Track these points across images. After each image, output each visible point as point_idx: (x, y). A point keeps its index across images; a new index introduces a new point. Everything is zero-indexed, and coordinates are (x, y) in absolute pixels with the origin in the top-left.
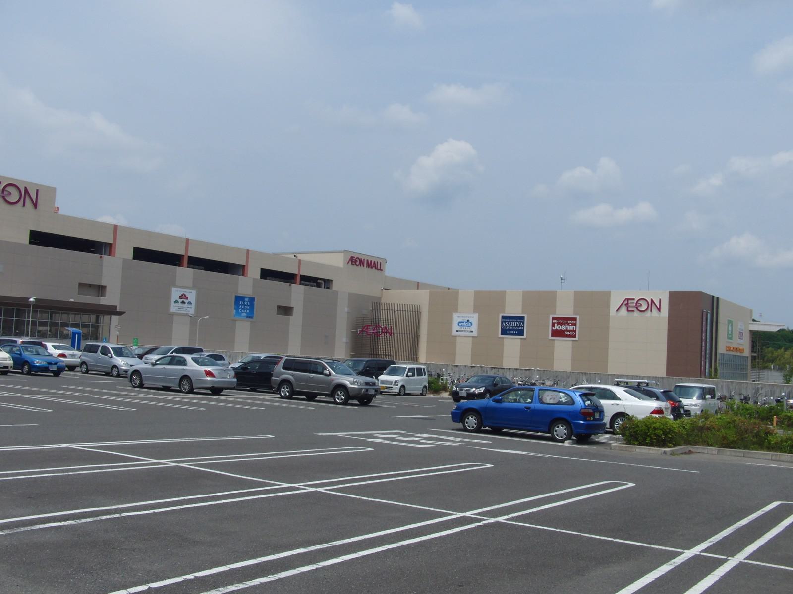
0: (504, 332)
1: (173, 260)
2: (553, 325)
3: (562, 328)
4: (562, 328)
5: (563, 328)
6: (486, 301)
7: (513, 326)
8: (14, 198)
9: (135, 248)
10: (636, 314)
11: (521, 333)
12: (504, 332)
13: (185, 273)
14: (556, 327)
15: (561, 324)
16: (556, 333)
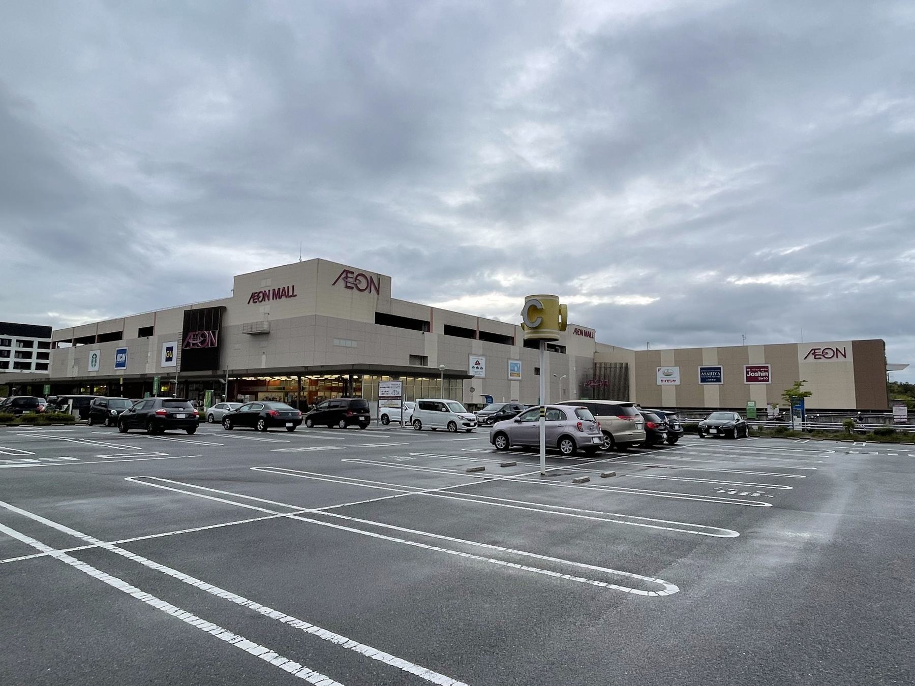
0: (703, 380)
1: (468, 333)
2: (747, 373)
3: (755, 374)
4: (755, 374)
5: (756, 374)
6: (682, 358)
7: (711, 375)
8: (363, 285)
9: (446, 326)
10: (823, 360)
11: (719, 380)
12: (703, 380)
13: (477, 343)
14: (750, 374)
15: (755, 372)
16: (750, 379)
